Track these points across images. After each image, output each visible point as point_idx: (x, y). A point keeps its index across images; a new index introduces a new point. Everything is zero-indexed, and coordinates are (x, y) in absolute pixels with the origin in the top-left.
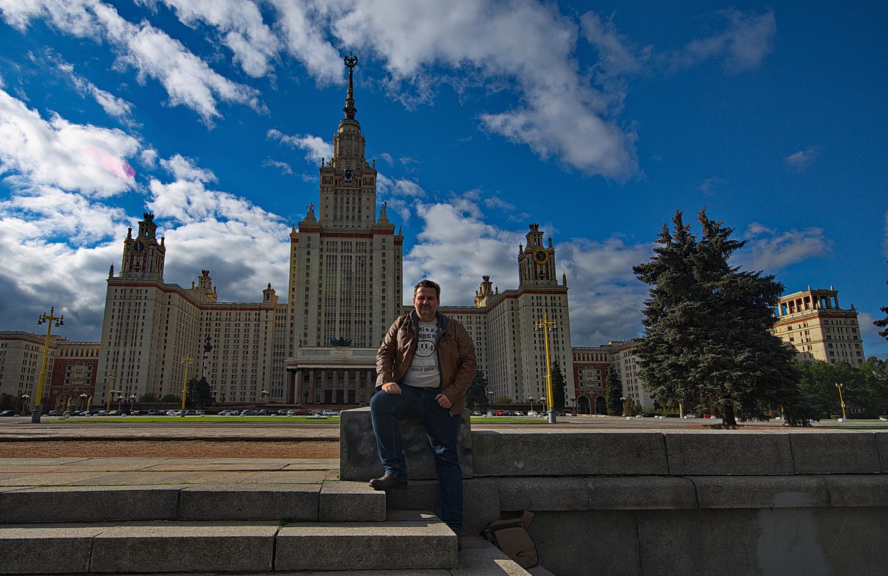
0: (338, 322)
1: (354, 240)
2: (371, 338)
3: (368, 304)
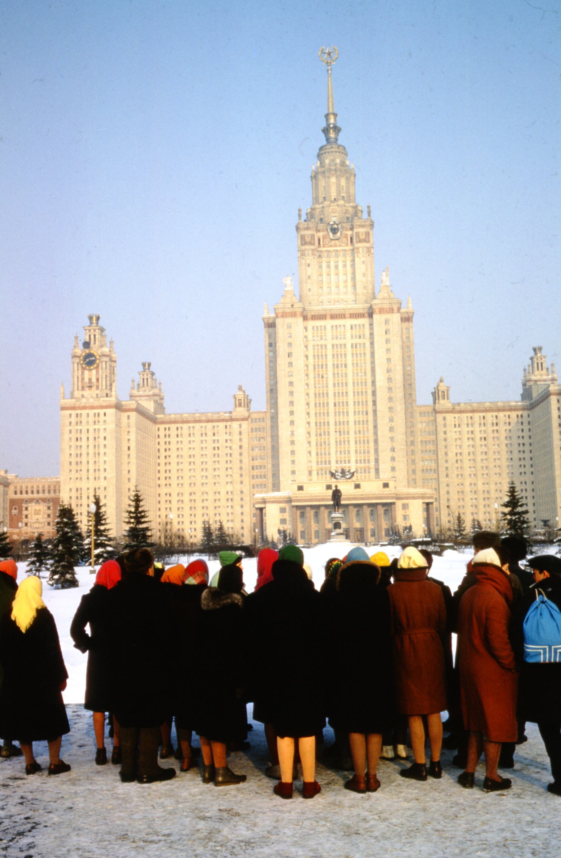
1: (348, 322)
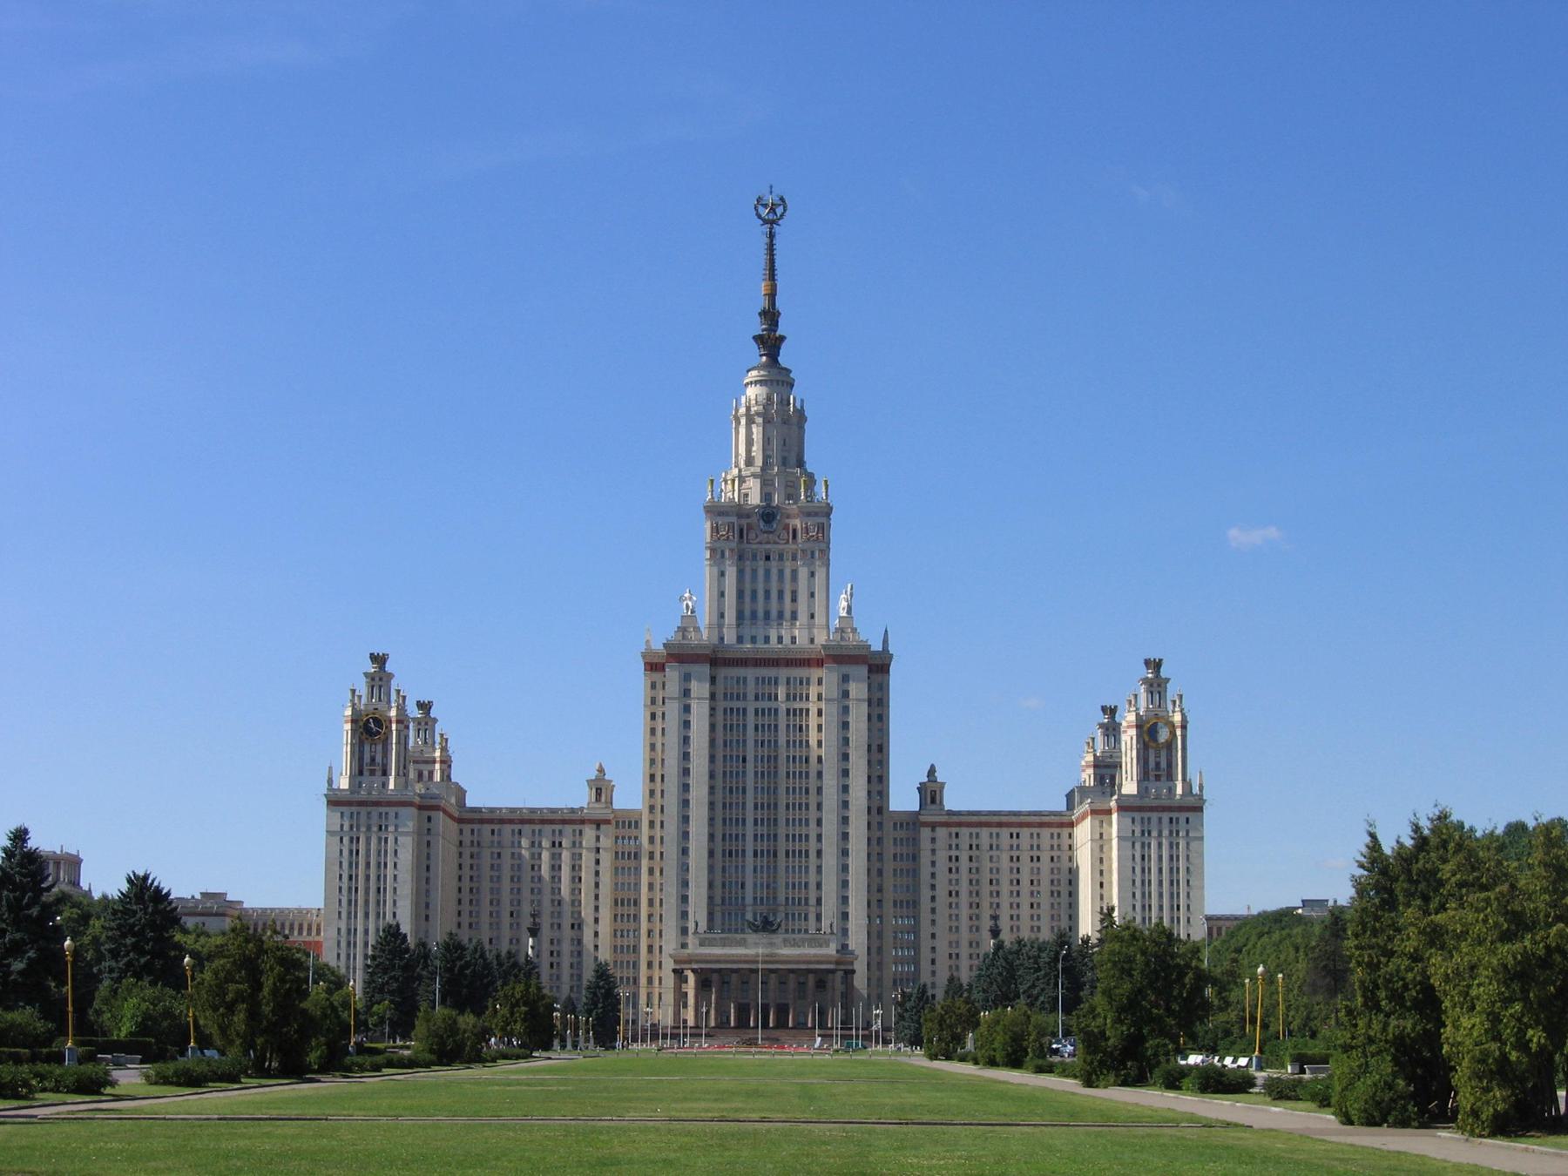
0: (750, 853)
3: (813, 814)
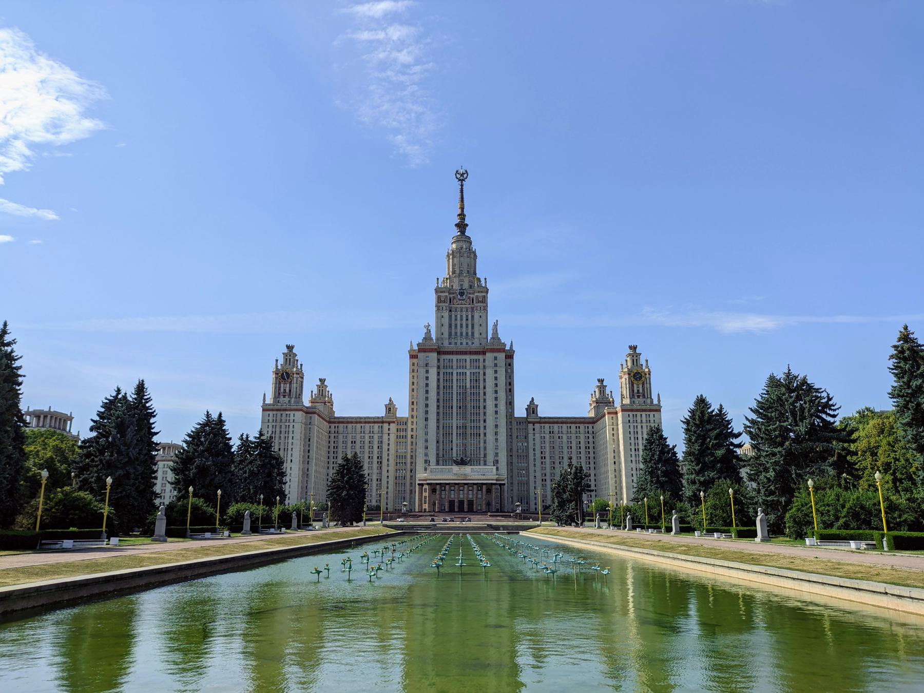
1: (468, 357)
2: (485, 449)
